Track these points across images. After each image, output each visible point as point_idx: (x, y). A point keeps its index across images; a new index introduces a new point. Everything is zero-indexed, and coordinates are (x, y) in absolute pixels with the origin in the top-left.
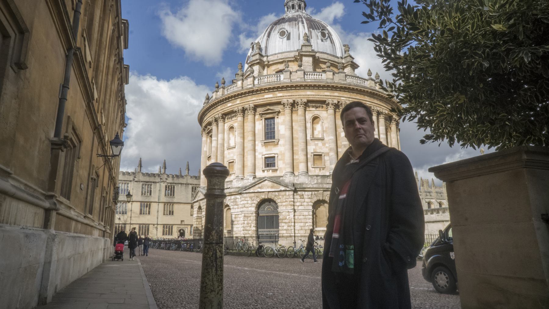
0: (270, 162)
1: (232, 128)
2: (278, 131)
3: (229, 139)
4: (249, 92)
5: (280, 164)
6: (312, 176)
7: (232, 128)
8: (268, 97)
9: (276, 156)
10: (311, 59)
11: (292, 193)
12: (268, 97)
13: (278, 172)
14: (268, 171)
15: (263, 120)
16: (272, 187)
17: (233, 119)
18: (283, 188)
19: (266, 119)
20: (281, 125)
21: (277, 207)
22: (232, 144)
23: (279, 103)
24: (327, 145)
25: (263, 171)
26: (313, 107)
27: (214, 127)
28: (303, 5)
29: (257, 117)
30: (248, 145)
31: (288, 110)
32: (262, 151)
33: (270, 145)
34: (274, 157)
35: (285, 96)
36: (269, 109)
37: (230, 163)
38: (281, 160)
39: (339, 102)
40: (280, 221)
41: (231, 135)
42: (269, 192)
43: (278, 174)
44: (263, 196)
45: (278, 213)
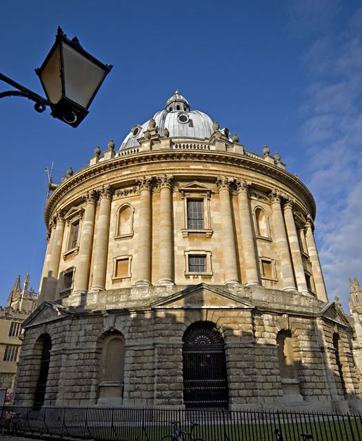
1: (123, 209)
2: (210, 218)
5: (212, 266)
8: (196, 168)
9: (209, 254)
11: (248, 314)
12: (196, 168)
13: (213, 279)
14: (195, 277)
15: (186, 200)
17: (129, 195)
19: (189, 200)
20: (216, 211)
22: (126, 230)
23: (213, 180)
25: (187, 276)
27: (88, 207)
30: (161, 232)
31: (224, 192)
33: (196, 237)
34: (205, 256)
36: (195, 186)
37: (117, 261)
38: (217, 261)
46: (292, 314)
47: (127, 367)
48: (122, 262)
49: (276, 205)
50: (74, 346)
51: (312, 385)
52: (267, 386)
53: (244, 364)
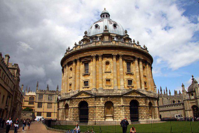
0: (86, 83)
1: (71, 69)
3: (70, 74)
4: (77, 52)
5: (90, 84)
6: (103, 90)
7: (71, 69)
8: (86, 54)
10: (108, 37)
12: (86, 54)
16: (86, 96)
18: (90, 96)
20: (92, 66)
21: (88, 105)
24: (113, 75)
25: (83, 88)
26: (106, 58)
27: (65, 69)
28: (108, 15)
29: (81, 63)
30: (77, 76)
31: (94, 60)
32: (83, 79)
35: (93, 54)
37: (70, 85)
38: (91, 82)
39: (118, 54)
40: (89, 112)
41: (71, 72)
42: (84, 98)
43: (89, 89)
44: (82, 100)
45: (88, 107)
46: (111, 97)
47: (69, 113)
48: (70, 85)
49: (115, 59)
50: (61, 108)
51: (116, 116)
52: (98, 117)
53: (92, 112)
